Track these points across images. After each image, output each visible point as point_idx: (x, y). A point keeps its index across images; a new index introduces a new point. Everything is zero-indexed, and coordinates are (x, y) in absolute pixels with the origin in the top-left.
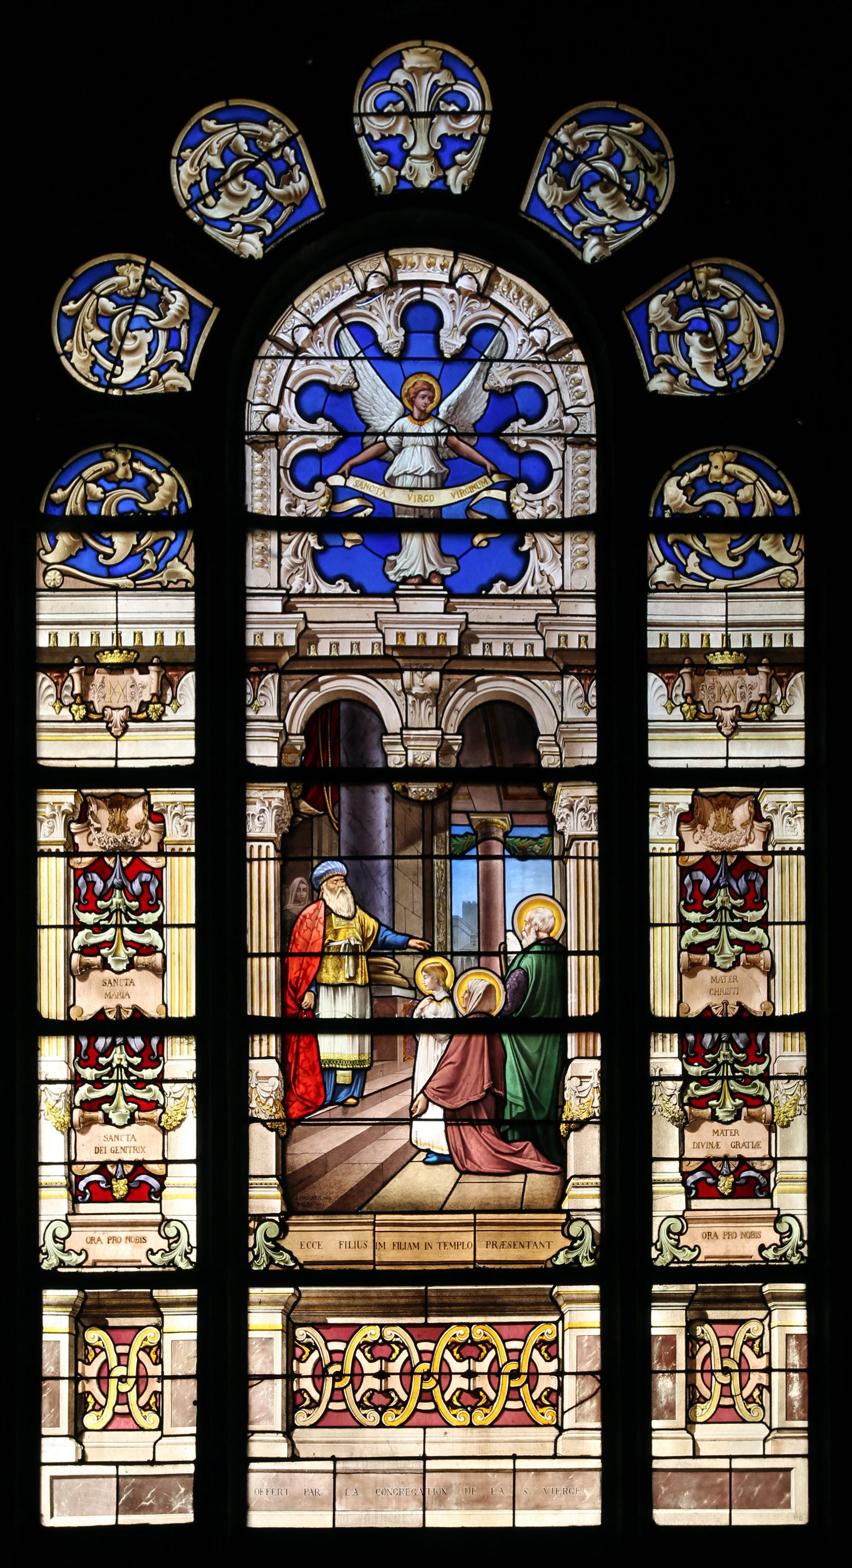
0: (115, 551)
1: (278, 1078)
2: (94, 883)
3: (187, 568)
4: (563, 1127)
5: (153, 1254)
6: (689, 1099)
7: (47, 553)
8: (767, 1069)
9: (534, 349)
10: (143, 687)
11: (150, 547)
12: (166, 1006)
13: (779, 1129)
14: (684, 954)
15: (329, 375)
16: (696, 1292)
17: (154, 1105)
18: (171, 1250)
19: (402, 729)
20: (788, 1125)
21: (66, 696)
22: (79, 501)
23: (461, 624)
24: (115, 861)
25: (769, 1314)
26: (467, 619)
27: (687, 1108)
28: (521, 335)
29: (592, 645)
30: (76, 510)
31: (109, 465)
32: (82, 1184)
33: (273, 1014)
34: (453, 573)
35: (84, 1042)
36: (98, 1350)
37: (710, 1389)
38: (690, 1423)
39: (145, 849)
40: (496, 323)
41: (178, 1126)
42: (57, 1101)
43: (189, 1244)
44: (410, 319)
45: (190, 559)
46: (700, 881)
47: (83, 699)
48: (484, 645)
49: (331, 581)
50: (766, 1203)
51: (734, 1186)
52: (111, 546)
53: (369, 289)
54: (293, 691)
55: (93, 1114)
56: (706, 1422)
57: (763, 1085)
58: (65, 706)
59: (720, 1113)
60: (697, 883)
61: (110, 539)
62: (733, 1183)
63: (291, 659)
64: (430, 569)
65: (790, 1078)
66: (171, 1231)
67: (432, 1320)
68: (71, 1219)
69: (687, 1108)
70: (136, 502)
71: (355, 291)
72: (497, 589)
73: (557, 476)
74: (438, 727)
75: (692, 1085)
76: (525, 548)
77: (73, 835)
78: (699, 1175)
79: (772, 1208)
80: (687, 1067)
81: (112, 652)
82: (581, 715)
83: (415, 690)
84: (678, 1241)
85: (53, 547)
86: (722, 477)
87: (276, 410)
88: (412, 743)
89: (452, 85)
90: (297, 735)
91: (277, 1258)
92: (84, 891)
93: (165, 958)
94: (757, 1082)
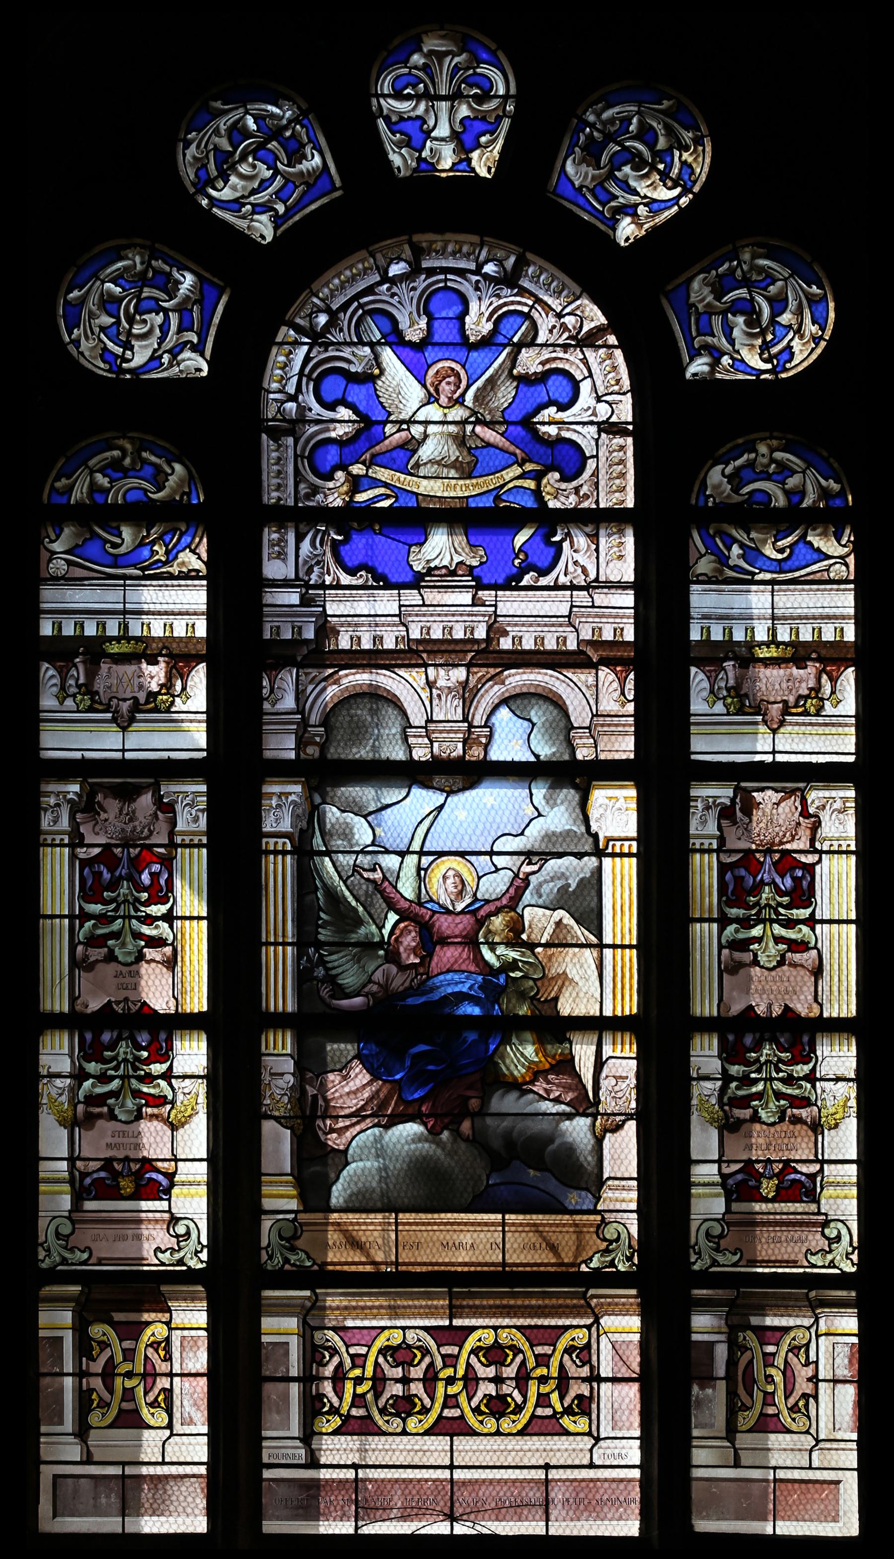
0: (123, 540)
1: (293, 1074)
2: (101, 873)
3: (199, 558)
5: (163, 1252)
6: (729, 1098)
7: (52, 541)
8: (813, 1070)
9: (566, 335)
10: (152, 678)
11: (161, 537)
12: (177, 1000)
13: (826, 1131)
14: (725, 952)
15: (349, 362)
16: (737, 1297)
17: (161, 1101)
18: (180, 1249)
19: (427, 721)
20: (836, 1126)
21: (70, 685)
22: (84, 490)
23: (490, 616)
24: (123, 852)
25: (817, 1321)
26: (495, 612)
27: (727, 1108)
28: (552, 320)
29: (629, 635)
30: (82, 498)
31: (116, 453)
32: (88, 1181)
33: (289, 1009)
34: (482, 563)
35: (89, 1036)
36: (103, 1346)
37: (752, 1396)
38: (731, 1432)
39: (154, 840)
40: (526, 309)
41: (186, 1123)
42: (61, 1095)
43: (199, 1243)
44: (433, 307)
45: (203, 550)
46: (743, 878)
47: (88, 689)
48: (513, 638)
49: (352, 572)
50: (813, 1207)
51: (778, 1188)
52: (119, 535)
53: (391, 274)
55: (97, 1110)
56: (749, 1431)
57: (809, 1086)
58: (68, 696)
59: (763, 1114)
60: (739, 880)
61: (118, 528)
62: (777, 1186)
63: (310, 652)
64: (457, 559)
65: (838, 1079)
66: (181, 1229)
67: (457, 1322)
68: (76, 1216)
69: (727, 1108)
70: (145, 491)
71: (378, 278)
72: (527, 580)
73: (591, 465)
75: (734, 1085)
76: (557, 538)
77: (78, 824)
78: (739, 1177)
79: (819, 1213)
80: (727, 1066)
81: (119, 643)
84: (718, 1244)
85: (58, 537)
86: (769, 465)
87: (293, 398)
89: (474, 68)
91: (293, 1258)
92: (90, 882)
93: (175, 951)
94: (803, 1083)
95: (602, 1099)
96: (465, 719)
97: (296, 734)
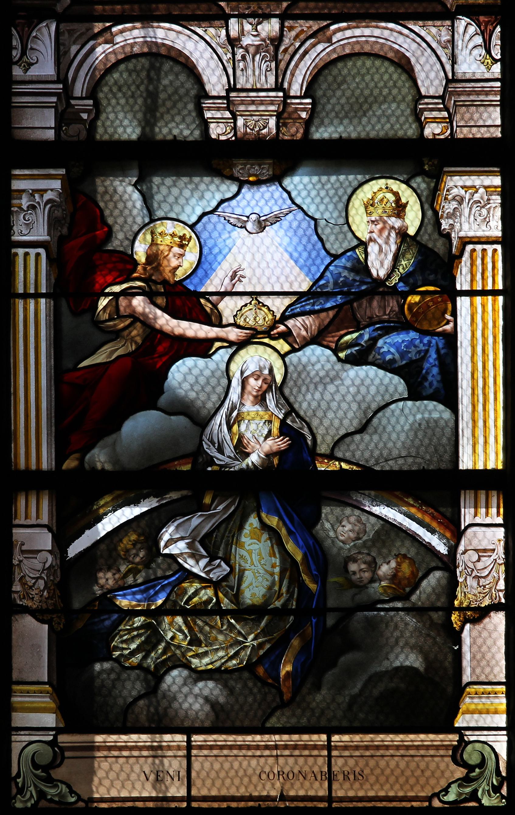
4: (455, 617)
19: (228, 91)
33: (45, 466)
54: (74, 43)
74: (278, 87)
82: (480, 71)
83: (247, 41)
88: (242, 108)
90: (81, 98)
91: (51, 791)
95: (460, 580)
96: (278, 87)
97: (56, 108)
